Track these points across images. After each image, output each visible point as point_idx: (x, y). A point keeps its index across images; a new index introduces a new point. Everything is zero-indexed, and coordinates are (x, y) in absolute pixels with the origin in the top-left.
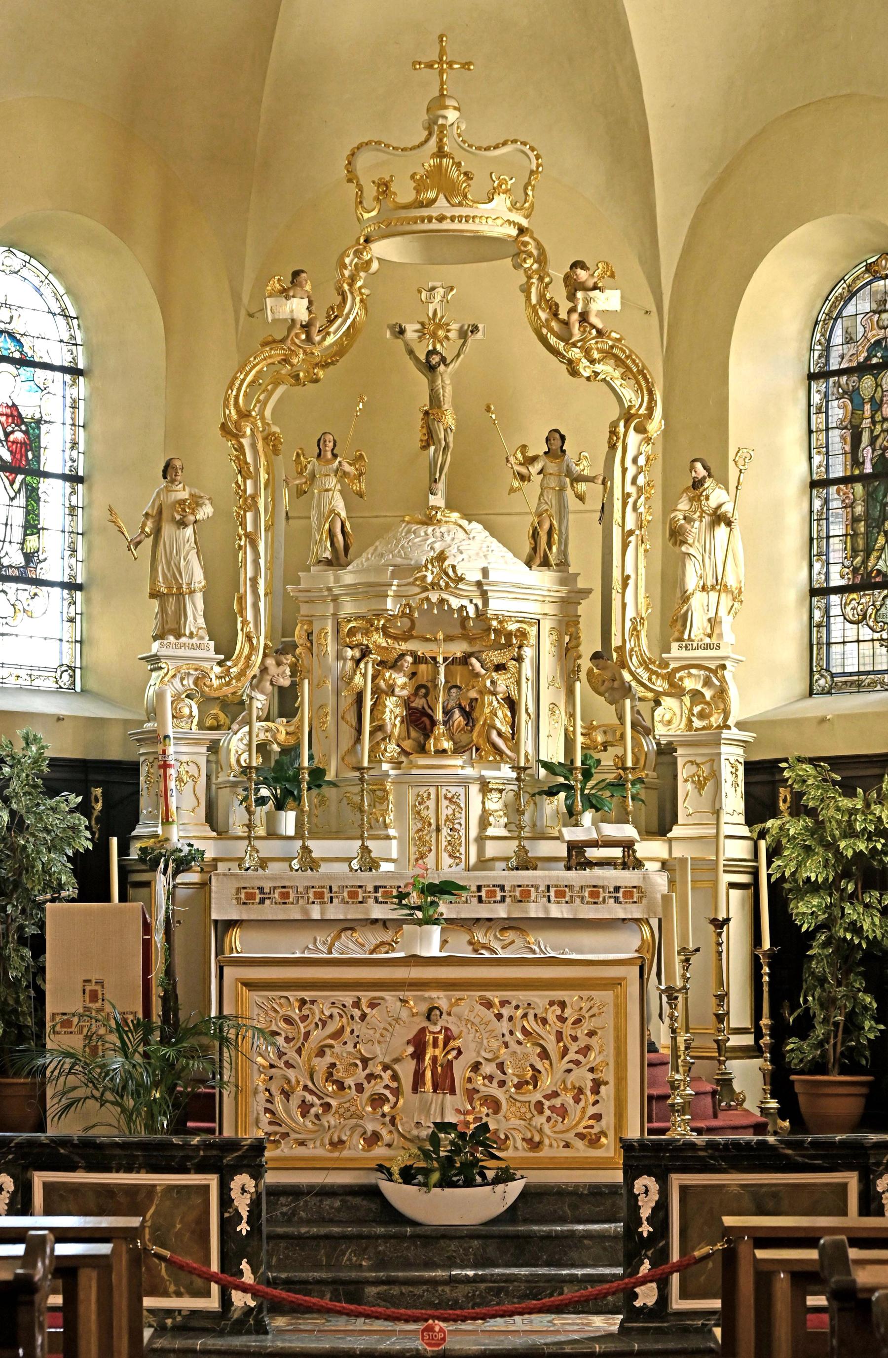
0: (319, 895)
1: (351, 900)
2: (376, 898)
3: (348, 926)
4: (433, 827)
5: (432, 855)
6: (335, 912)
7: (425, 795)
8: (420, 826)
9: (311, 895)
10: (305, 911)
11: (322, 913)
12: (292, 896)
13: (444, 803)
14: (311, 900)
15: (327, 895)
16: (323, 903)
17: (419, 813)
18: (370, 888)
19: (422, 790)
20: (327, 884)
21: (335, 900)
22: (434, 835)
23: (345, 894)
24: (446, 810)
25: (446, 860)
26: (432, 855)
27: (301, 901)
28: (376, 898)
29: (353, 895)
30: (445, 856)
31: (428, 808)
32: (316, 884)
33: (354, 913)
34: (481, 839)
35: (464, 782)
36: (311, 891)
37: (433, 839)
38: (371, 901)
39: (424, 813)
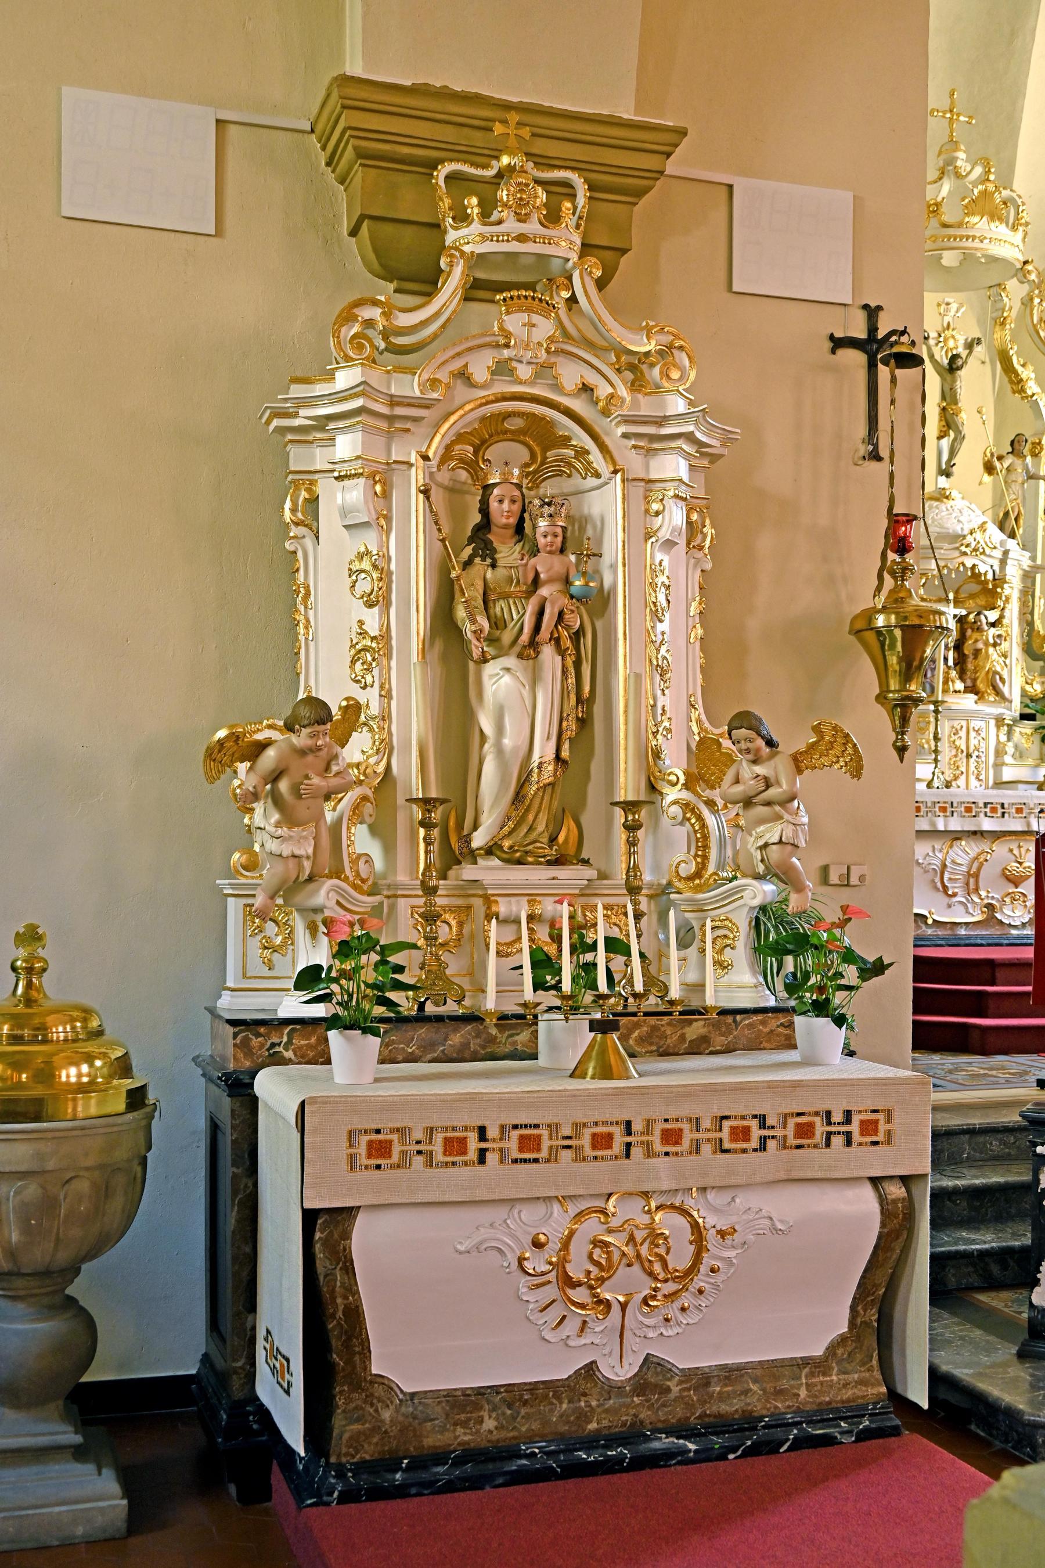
0: (943, 809)
1: (967, 814)
2: (986, 813)
3: (956, 836)
4: (965, 754)
5: (963, 777)
6: (955, 824)
7: (959, 727)
8: (954, 752)
9: (937, 809)
10: (933, 824)
11: (946, 826)
12: (923, 809)
13: (972, 734)
14: (938, 813)
15: (949, 809)
16: (946, 816)
17: (954, 742)
18: (981, 805)
19: (956, 723)
20: (949, 801)
21: (955, 814)
22: (965, 760)
23: (963, 809)
24: (973, 742)
25: (973, 782)
26: (963, 777)
27: (930, 814)
28: (986, 813)
29: (968, 810)
30: (972, 778)
31: (960, 738)
32: (941, 800)
33: (969, 825)
34: (998, 765)
35: (984, 717)
36: (938, 805)
37: (964, 764)
38: (982, 815)
39: (957, 743)
